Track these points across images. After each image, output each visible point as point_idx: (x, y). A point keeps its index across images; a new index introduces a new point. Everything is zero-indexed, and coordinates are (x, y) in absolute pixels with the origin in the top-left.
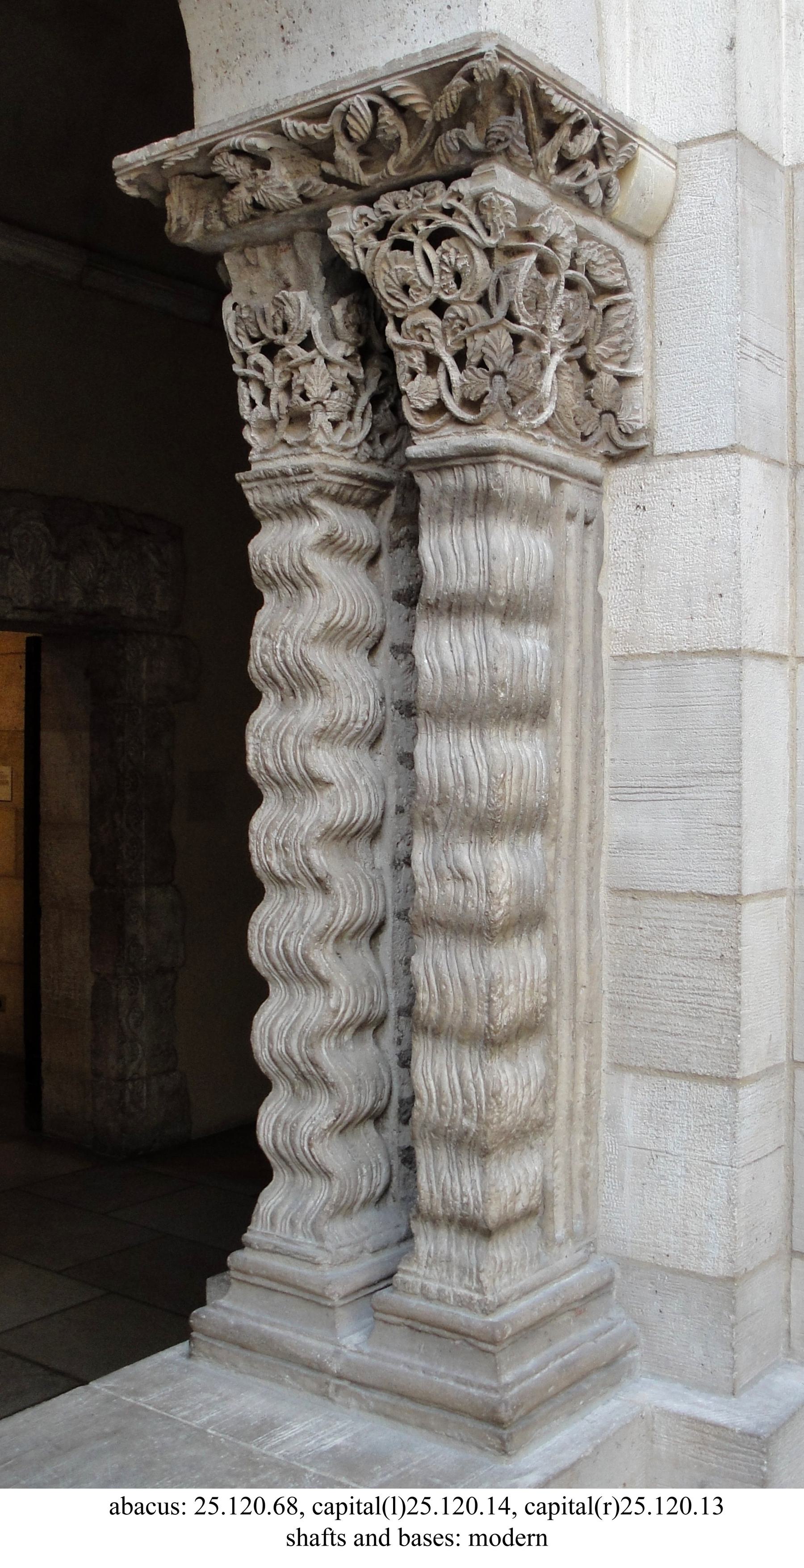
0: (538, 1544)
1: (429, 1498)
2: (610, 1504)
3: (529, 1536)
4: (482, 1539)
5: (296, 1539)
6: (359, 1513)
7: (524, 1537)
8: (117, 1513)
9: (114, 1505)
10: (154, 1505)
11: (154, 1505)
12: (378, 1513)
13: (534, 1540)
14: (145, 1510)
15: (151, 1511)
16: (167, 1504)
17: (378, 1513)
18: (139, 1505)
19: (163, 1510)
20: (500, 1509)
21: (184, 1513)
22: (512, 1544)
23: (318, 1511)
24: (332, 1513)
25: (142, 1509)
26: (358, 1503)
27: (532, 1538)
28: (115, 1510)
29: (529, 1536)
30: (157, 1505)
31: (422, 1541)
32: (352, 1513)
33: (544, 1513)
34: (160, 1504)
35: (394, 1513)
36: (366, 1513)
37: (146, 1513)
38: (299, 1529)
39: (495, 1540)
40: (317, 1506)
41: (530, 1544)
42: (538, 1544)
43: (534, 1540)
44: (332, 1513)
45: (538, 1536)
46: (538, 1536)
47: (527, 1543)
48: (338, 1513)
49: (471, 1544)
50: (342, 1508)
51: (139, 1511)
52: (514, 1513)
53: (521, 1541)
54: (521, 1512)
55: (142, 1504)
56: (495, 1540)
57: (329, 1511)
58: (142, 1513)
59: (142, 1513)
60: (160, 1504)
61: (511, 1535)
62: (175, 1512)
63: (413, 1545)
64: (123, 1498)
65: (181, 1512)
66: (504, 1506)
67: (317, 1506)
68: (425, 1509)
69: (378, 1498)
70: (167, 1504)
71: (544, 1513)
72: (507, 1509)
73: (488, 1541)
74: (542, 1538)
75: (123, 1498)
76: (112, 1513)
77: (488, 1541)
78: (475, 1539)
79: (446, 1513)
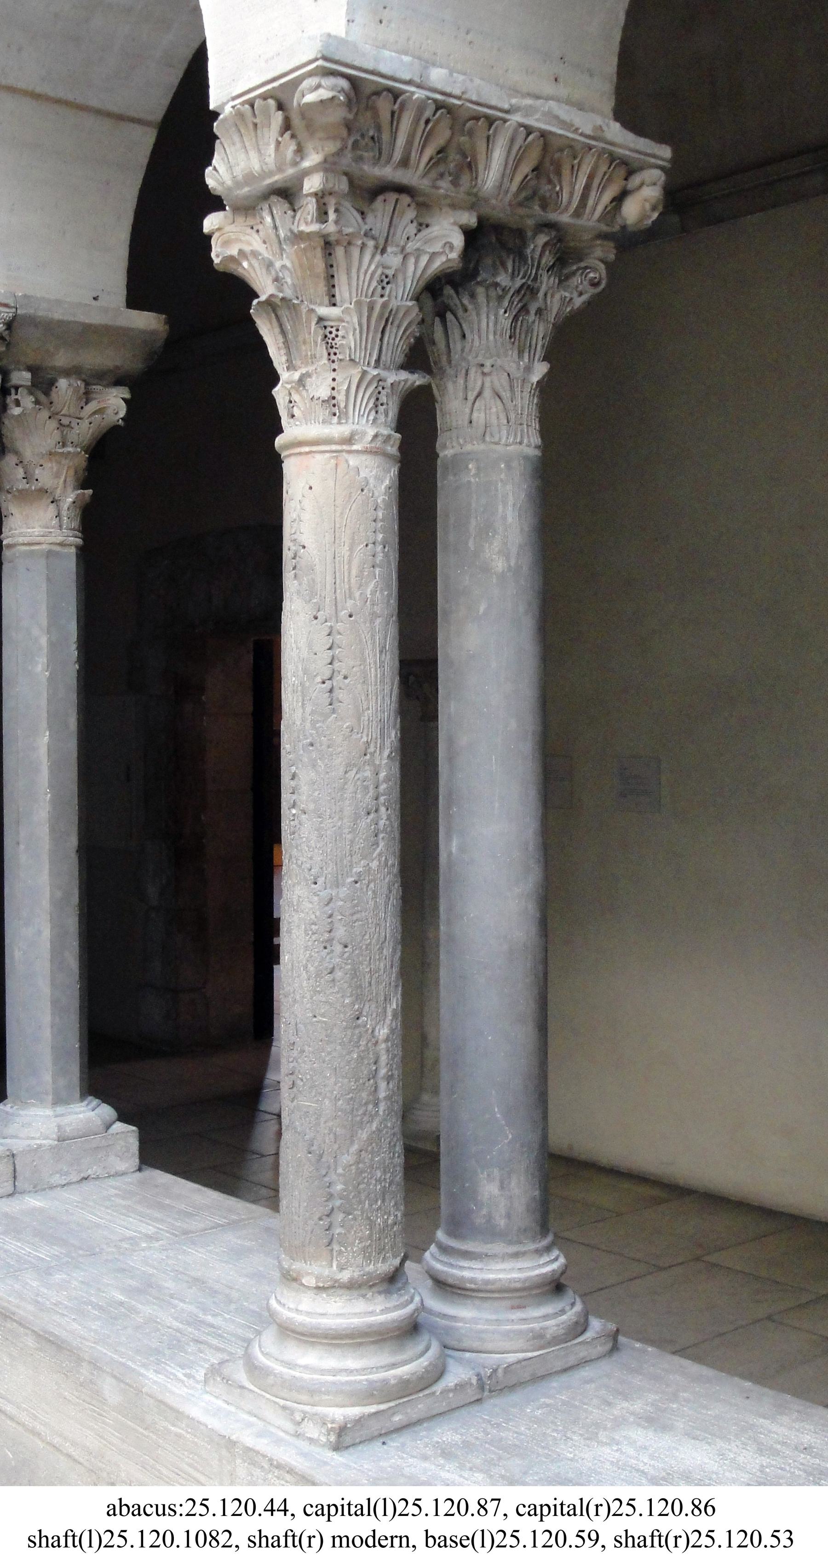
0: (401, 1546)
1: (420, 1500)
2: (601, 1505)
3: (392, 1537)
4: (344, 1540)
7: (387, 1539)
13: (396, 1541)
20: (265, 1510)
22: (374, 1546)
23: (521, 1513)
24: (323, 1515)
27: (395, 1539)
29: (392, 1537)
31: (449, 1542)
32: (343, 1515)
33: (535, 1514)
34: (157, 1506)
35: (385, 1515)
39: (358, 1542)
41: (392, 1546)
42: (401, 1546)
43: (396, 1541)
44: (323, 1515)
45: (401, 1537)
46: (401, 1537)
47: (390, 1545)
49: (334, 1546)
52: (293, 1515)
53: (383, 1543)
54: (512, 1513)
56: (358, 1542)
57: (320, 1512)
60: (157, 1506)
61: (374, 1537)
63: (439, 1546)
66: (269, 1508)
69: (581, 1499)
71: (535, 1514)
72: (285, 1511)
73: (350, 1542)
74: (404, 1540)
77: (350, 1542)
78: (337, 1540)
79: (437, 1515)
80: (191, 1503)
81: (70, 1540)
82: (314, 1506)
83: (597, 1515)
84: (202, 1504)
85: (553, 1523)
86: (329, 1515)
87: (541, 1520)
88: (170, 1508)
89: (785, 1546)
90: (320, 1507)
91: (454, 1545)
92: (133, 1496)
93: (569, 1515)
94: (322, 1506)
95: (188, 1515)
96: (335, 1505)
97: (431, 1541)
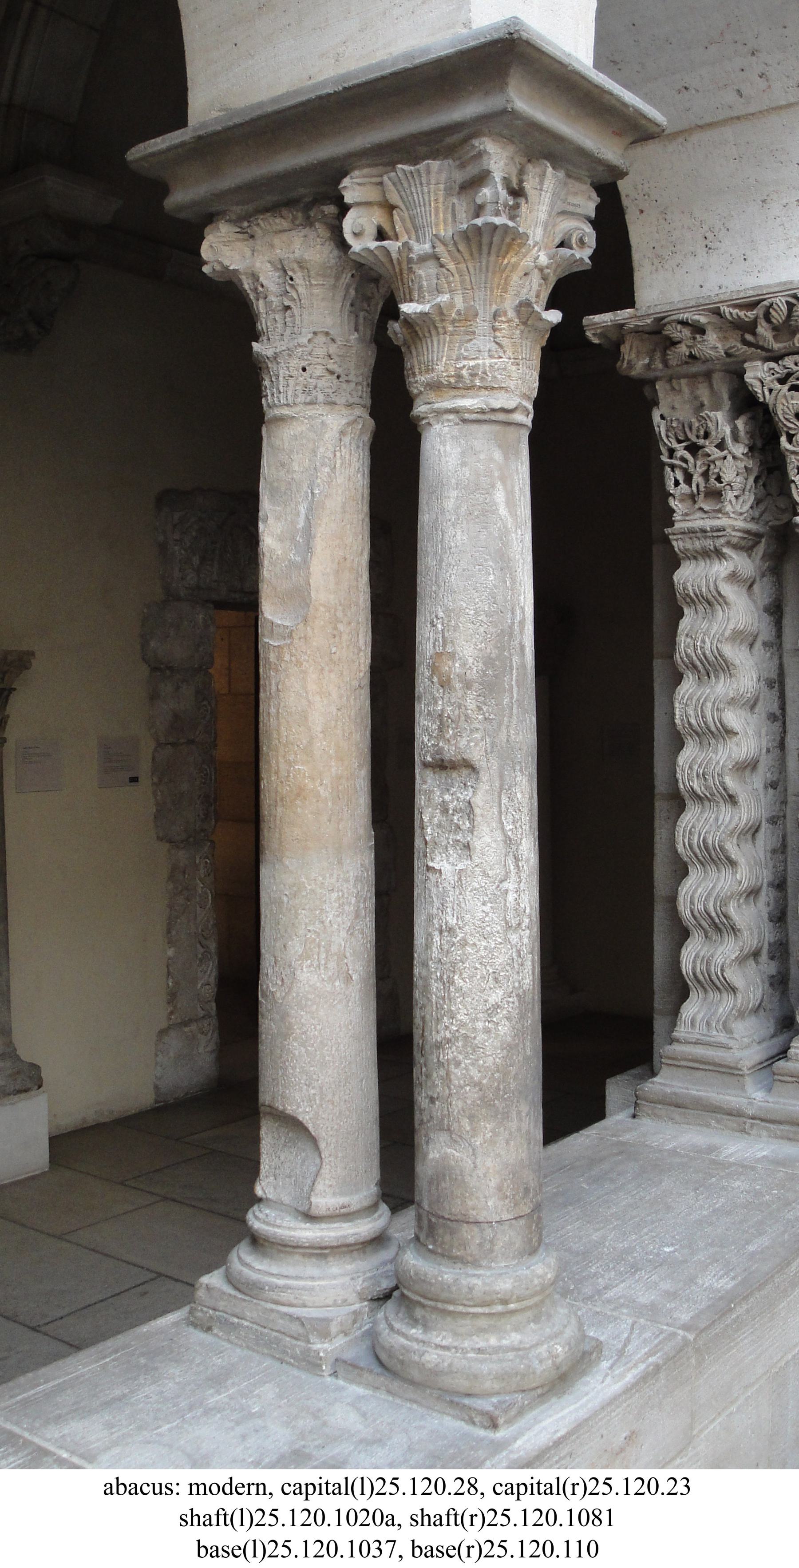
5: (189, 1519)
6: (328, 1494)
10: (148, 1485)
11: (148, 1485)
14: (139, 1491)
15: (145, 1492)
16: (161, 1485)
17: (347, 1494)
18: (133, 1486)
19: (157, 1490)
21: (178, 1494)
25: (136, 1490)
26: (327, 1483)
28: (108, 1490)
36: (334, 1494)
37: (140, 1494)
38: (192, 1510)
40: (286, 1486)
58: (136, 1493)
62: (169, 1492)
64: (117, 1478)
65: (174, 1493)
67: (286, 1486)
68: (393, 1489)
70: (161, 1485)
75: (117, 1478)
83: (574, 1494)
86: (307, 1494)
88: (166, 1487)
92: (128, 1476)
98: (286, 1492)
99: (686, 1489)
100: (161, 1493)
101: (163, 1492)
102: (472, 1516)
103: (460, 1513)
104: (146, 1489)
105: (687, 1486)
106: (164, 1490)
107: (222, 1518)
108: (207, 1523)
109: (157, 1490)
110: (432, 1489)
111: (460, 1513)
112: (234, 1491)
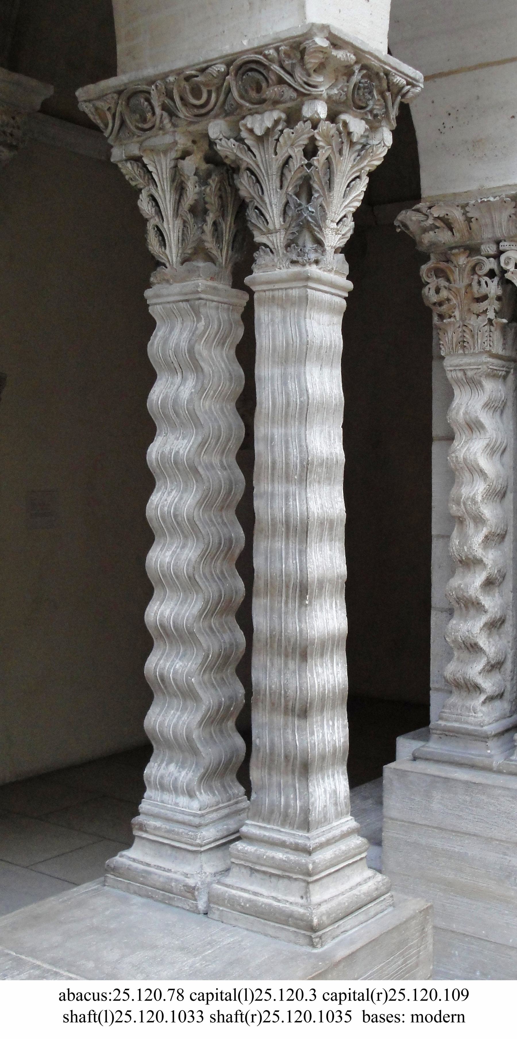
8: (64, 1000)
9: (62, 994)
10: (90, 994)
11: (90, 994)
12: (235, 1000)
14: (83, 998)
15: (88, 999)
18: (79, 994)
19: (96, 998)
24: (203, 1000)
30: (92, 994)
32: (217, 1000)
34: (94, 994)
37: (84, 1000)
40: (193, 995)
44: (203, 1000)
48: (208, 1000)
50: (210, 996)
51: (79, 998)
55: (81, 994)
57: (201, 998)
58: (81, 1000)
59: (81, 1000)
60: (94, 994)
64: (68, 989)
75: (68, 989)
76: (60, 1000)
80: (117, 991)
81: (92, 1017)
82: (197, 994)
84: (124, 993)
85: (346, 1005)
87: (340, 1004)
89: (346, 1022)
90: (201, 994)
91: (382, 1020)
93: (359, 1000)
94: (203, 994)
95: (115, 1000)
96: (211, 993)
97: (367, 1018)
98: (193, 999)
99: (313, 996)
100: (98, 1000)
101: (100, 999)
102: (253, 1015)
103: (244, 1013)
104: (88, 997)
105: (314, 995)
106: (101, 997)
107: (239, 1017)
108: (229, 1020)
109: (96, 998)
110: (294, 996)
111: (244, 1013)
112: (83, 998)
